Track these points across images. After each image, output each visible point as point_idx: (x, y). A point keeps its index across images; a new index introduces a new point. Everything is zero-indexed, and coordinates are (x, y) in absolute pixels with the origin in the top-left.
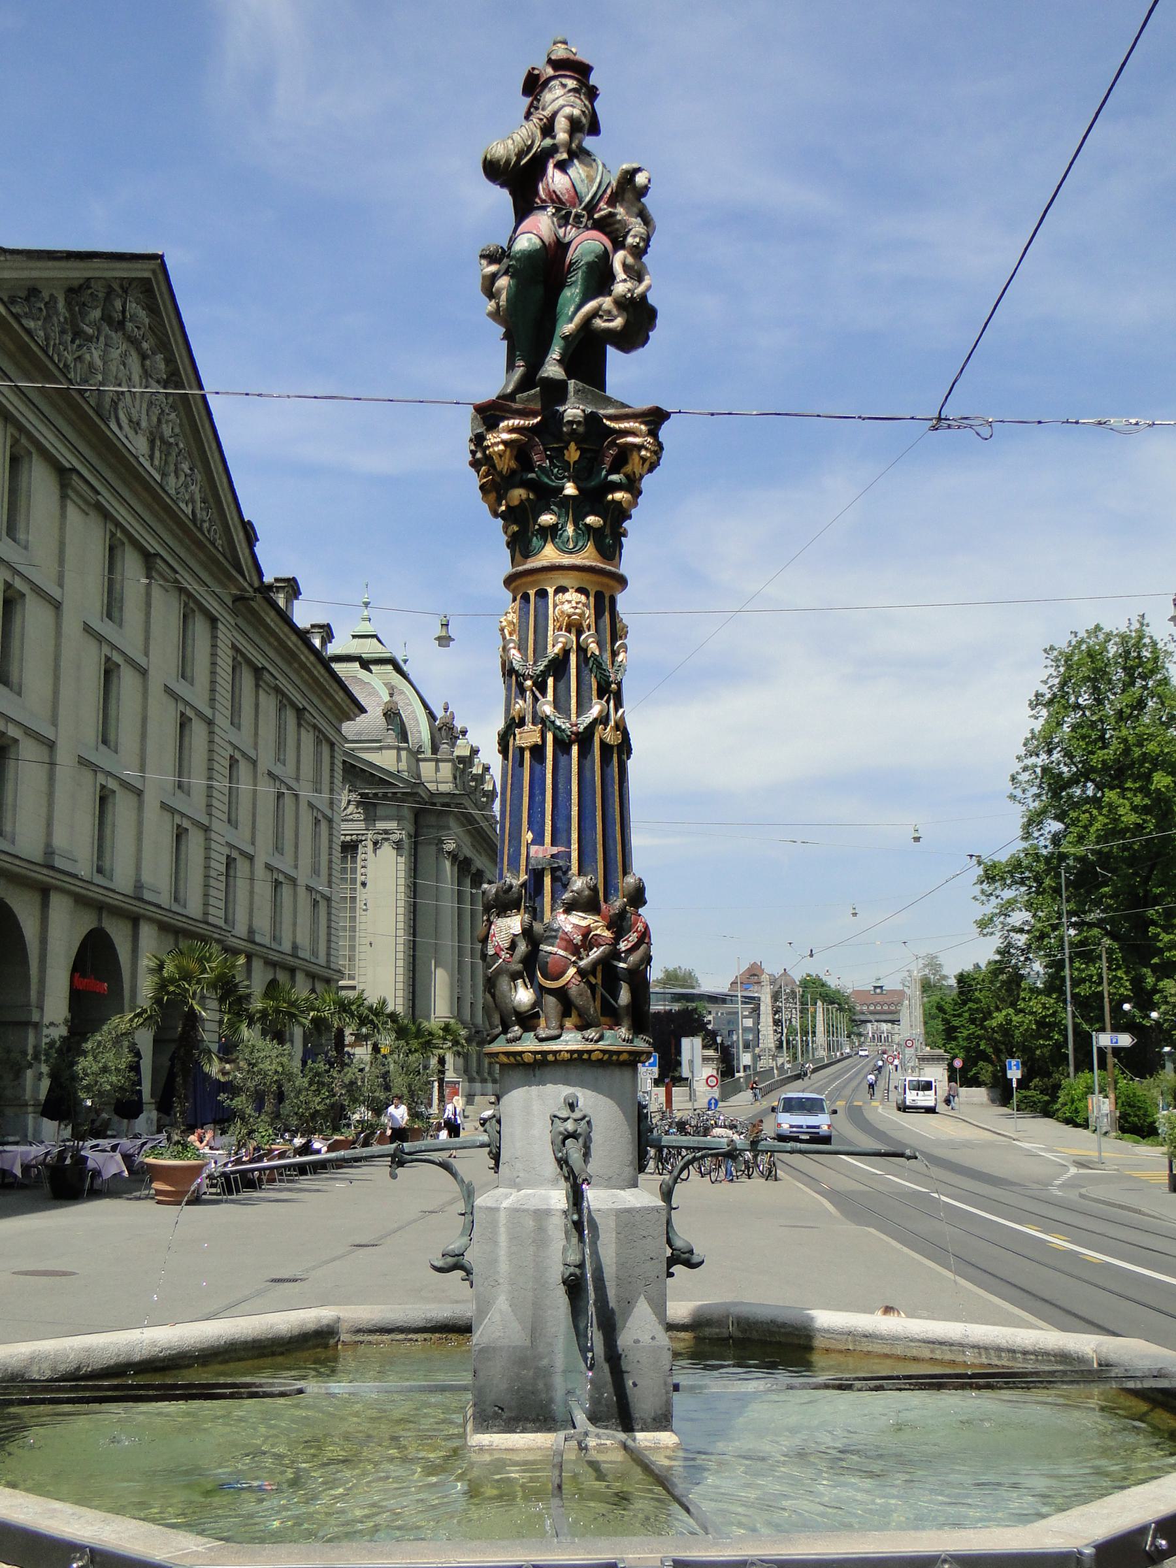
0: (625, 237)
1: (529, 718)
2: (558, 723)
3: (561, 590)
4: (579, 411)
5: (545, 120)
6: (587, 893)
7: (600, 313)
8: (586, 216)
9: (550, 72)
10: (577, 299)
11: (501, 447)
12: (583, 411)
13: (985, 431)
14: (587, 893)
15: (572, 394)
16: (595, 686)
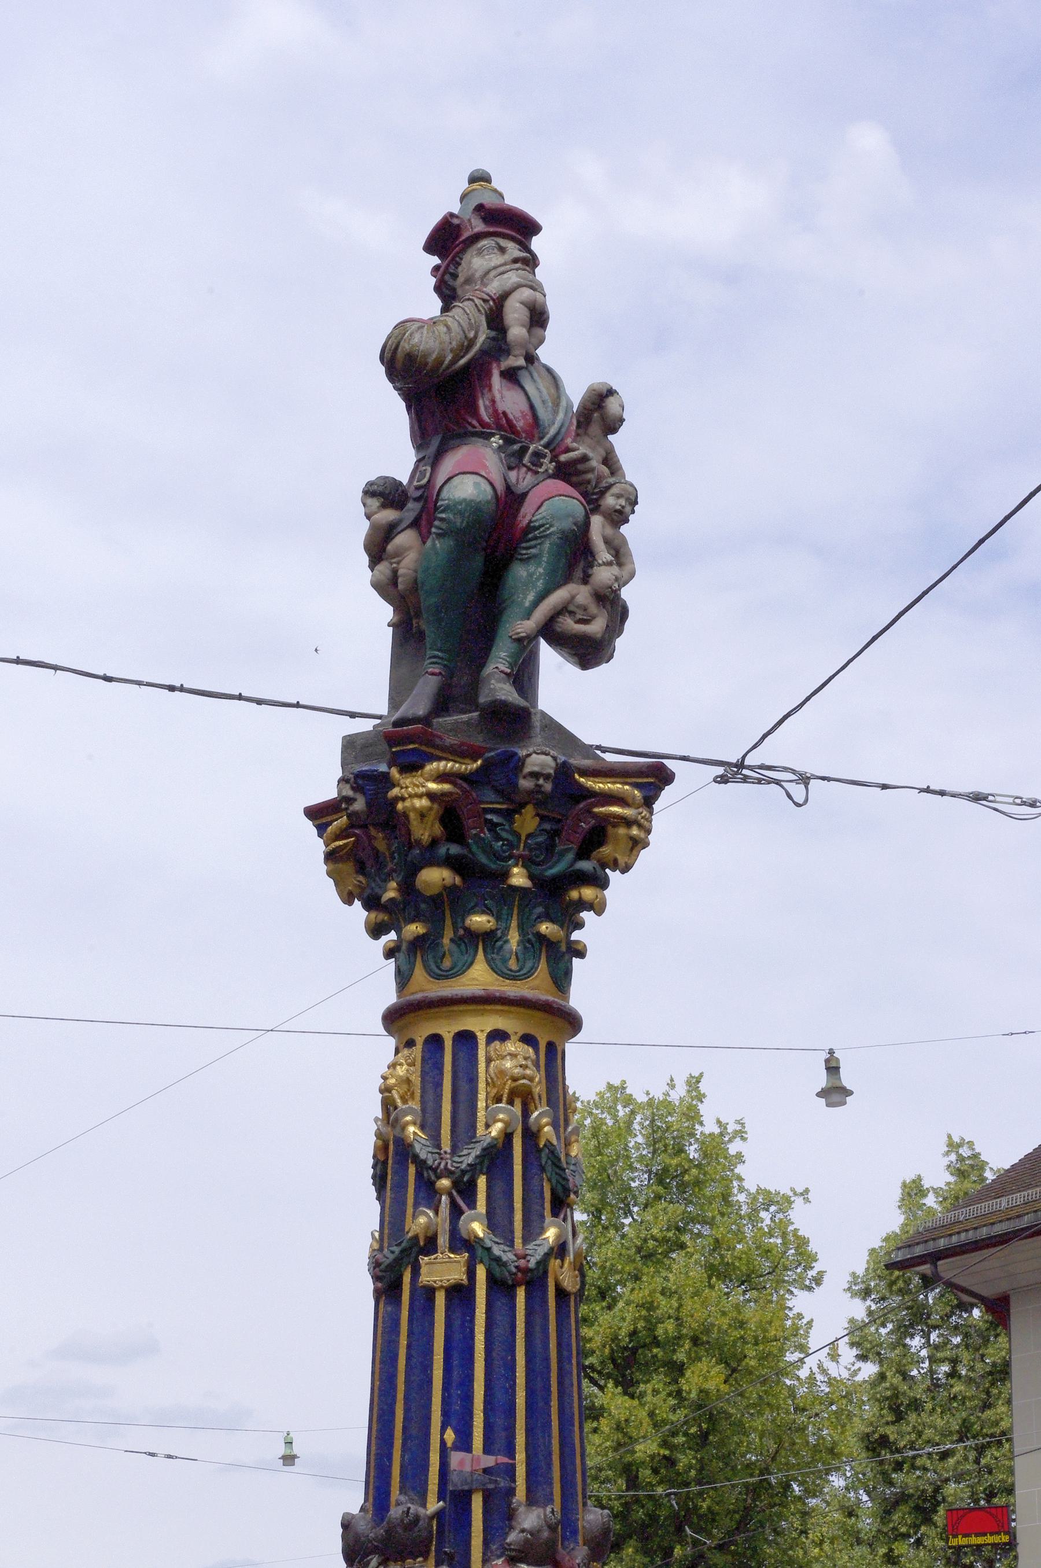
0: (603, 493)
1: (443, 1240)
2: (497, 1251)
3: (498, 1036)
4: (548, 759)
5: (491, 303)
6: (546, 1534)
7: (571, 608)
8: (549, 455)
9: (479, 226)
10: (540, 584)
11: (424, 802)
12: (555, 758)
13: (798, 791)
14: (546, 1534)
15: (538, 730)
16: (547, 1195)
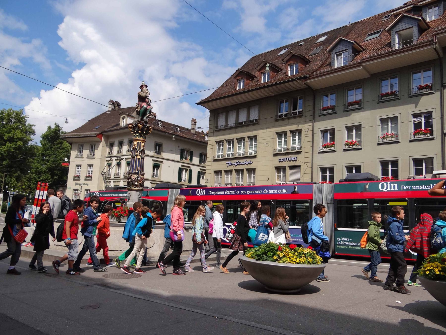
3: (142, 142)
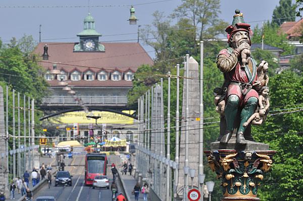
11: (226, 164)
